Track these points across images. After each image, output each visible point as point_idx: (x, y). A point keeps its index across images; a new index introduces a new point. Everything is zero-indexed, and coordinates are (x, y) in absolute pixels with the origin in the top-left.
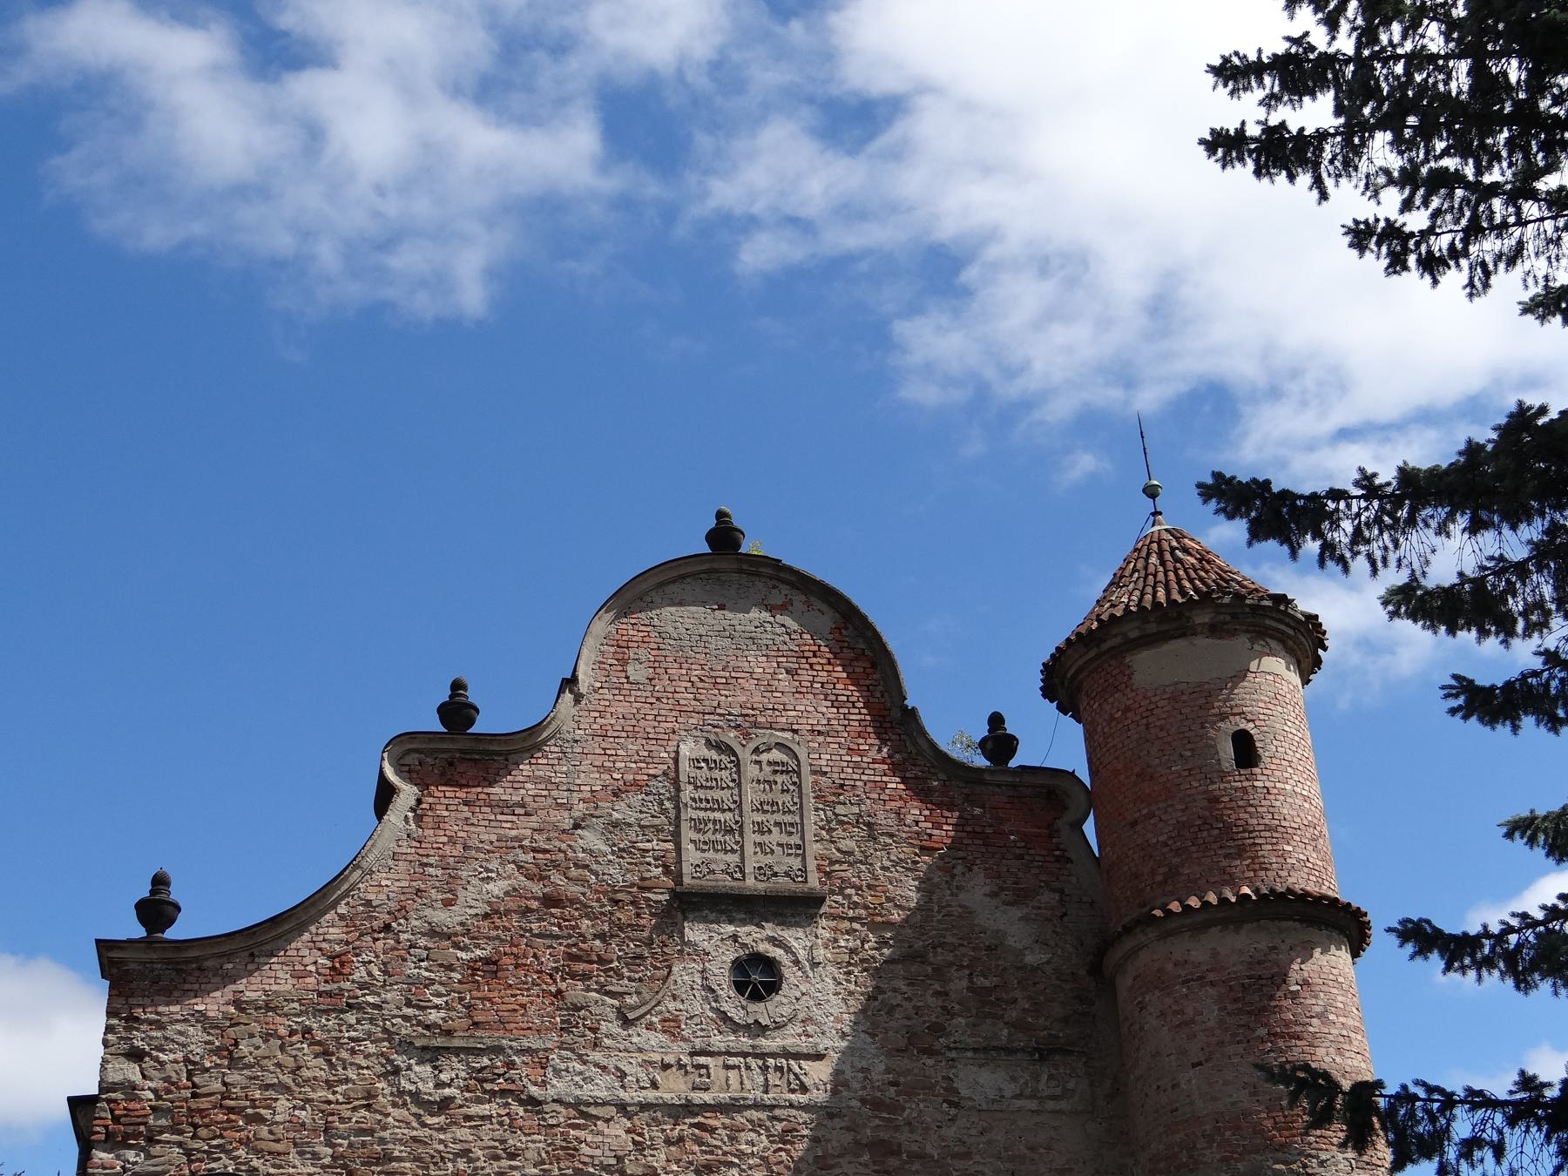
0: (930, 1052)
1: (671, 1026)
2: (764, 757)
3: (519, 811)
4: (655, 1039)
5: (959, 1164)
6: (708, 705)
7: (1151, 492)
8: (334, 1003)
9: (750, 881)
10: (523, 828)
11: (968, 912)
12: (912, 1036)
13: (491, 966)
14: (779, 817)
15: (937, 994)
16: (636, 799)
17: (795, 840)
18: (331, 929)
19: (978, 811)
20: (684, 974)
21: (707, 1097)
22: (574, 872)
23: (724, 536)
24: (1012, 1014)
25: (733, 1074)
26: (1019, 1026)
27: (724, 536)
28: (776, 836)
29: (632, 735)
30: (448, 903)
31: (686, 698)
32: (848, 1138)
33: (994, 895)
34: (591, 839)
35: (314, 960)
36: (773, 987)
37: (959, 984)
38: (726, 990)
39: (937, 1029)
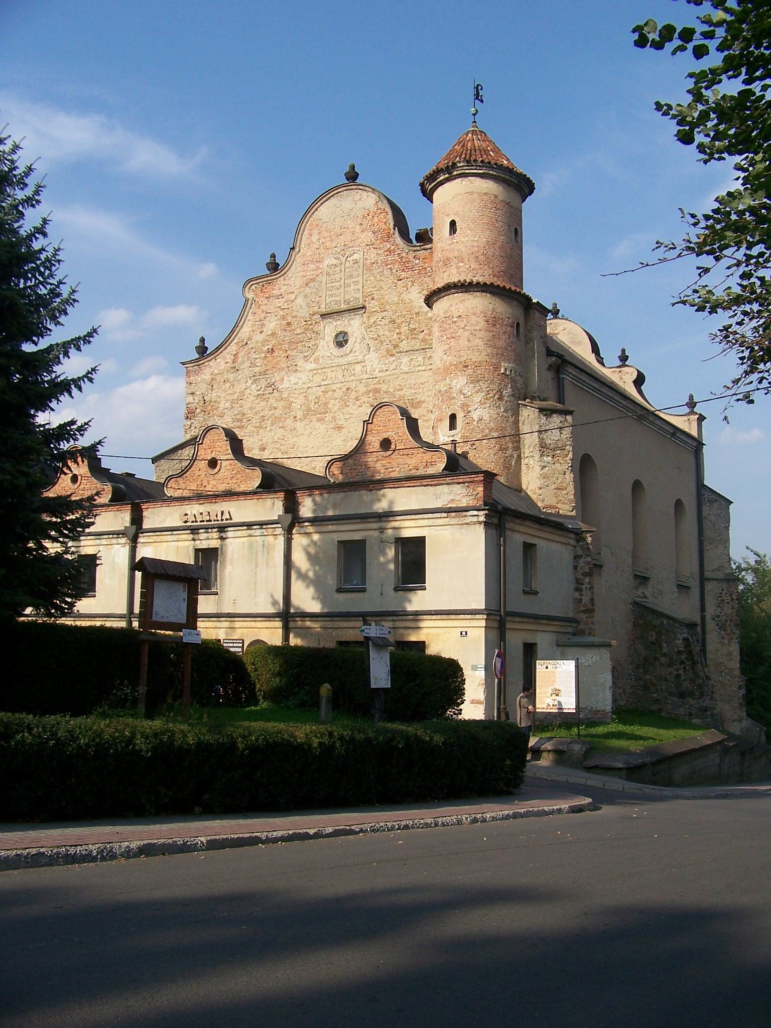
0: (392, 355)
1: (316, 361)
5: (398, 393)
6: (335, 244)
8: (235, 369)
10: (279, 303)
11: (411, 301)
12: (388, 351)
14: (355, 280)
16: (312, 284)
18: (233, 348)
19: (417, 261)
20: (322, 343)
22: (295, 313)
25: (334, 374)
26: (424, 340)
28: (353, 287)
29: (312, 262)
31: (328, 244)
32: (365, 389)
33: (420, 293)
34: (300, 301)
35: (230, 358)
36: (346, 341)
37: (404, 329)
38: (332, 345)
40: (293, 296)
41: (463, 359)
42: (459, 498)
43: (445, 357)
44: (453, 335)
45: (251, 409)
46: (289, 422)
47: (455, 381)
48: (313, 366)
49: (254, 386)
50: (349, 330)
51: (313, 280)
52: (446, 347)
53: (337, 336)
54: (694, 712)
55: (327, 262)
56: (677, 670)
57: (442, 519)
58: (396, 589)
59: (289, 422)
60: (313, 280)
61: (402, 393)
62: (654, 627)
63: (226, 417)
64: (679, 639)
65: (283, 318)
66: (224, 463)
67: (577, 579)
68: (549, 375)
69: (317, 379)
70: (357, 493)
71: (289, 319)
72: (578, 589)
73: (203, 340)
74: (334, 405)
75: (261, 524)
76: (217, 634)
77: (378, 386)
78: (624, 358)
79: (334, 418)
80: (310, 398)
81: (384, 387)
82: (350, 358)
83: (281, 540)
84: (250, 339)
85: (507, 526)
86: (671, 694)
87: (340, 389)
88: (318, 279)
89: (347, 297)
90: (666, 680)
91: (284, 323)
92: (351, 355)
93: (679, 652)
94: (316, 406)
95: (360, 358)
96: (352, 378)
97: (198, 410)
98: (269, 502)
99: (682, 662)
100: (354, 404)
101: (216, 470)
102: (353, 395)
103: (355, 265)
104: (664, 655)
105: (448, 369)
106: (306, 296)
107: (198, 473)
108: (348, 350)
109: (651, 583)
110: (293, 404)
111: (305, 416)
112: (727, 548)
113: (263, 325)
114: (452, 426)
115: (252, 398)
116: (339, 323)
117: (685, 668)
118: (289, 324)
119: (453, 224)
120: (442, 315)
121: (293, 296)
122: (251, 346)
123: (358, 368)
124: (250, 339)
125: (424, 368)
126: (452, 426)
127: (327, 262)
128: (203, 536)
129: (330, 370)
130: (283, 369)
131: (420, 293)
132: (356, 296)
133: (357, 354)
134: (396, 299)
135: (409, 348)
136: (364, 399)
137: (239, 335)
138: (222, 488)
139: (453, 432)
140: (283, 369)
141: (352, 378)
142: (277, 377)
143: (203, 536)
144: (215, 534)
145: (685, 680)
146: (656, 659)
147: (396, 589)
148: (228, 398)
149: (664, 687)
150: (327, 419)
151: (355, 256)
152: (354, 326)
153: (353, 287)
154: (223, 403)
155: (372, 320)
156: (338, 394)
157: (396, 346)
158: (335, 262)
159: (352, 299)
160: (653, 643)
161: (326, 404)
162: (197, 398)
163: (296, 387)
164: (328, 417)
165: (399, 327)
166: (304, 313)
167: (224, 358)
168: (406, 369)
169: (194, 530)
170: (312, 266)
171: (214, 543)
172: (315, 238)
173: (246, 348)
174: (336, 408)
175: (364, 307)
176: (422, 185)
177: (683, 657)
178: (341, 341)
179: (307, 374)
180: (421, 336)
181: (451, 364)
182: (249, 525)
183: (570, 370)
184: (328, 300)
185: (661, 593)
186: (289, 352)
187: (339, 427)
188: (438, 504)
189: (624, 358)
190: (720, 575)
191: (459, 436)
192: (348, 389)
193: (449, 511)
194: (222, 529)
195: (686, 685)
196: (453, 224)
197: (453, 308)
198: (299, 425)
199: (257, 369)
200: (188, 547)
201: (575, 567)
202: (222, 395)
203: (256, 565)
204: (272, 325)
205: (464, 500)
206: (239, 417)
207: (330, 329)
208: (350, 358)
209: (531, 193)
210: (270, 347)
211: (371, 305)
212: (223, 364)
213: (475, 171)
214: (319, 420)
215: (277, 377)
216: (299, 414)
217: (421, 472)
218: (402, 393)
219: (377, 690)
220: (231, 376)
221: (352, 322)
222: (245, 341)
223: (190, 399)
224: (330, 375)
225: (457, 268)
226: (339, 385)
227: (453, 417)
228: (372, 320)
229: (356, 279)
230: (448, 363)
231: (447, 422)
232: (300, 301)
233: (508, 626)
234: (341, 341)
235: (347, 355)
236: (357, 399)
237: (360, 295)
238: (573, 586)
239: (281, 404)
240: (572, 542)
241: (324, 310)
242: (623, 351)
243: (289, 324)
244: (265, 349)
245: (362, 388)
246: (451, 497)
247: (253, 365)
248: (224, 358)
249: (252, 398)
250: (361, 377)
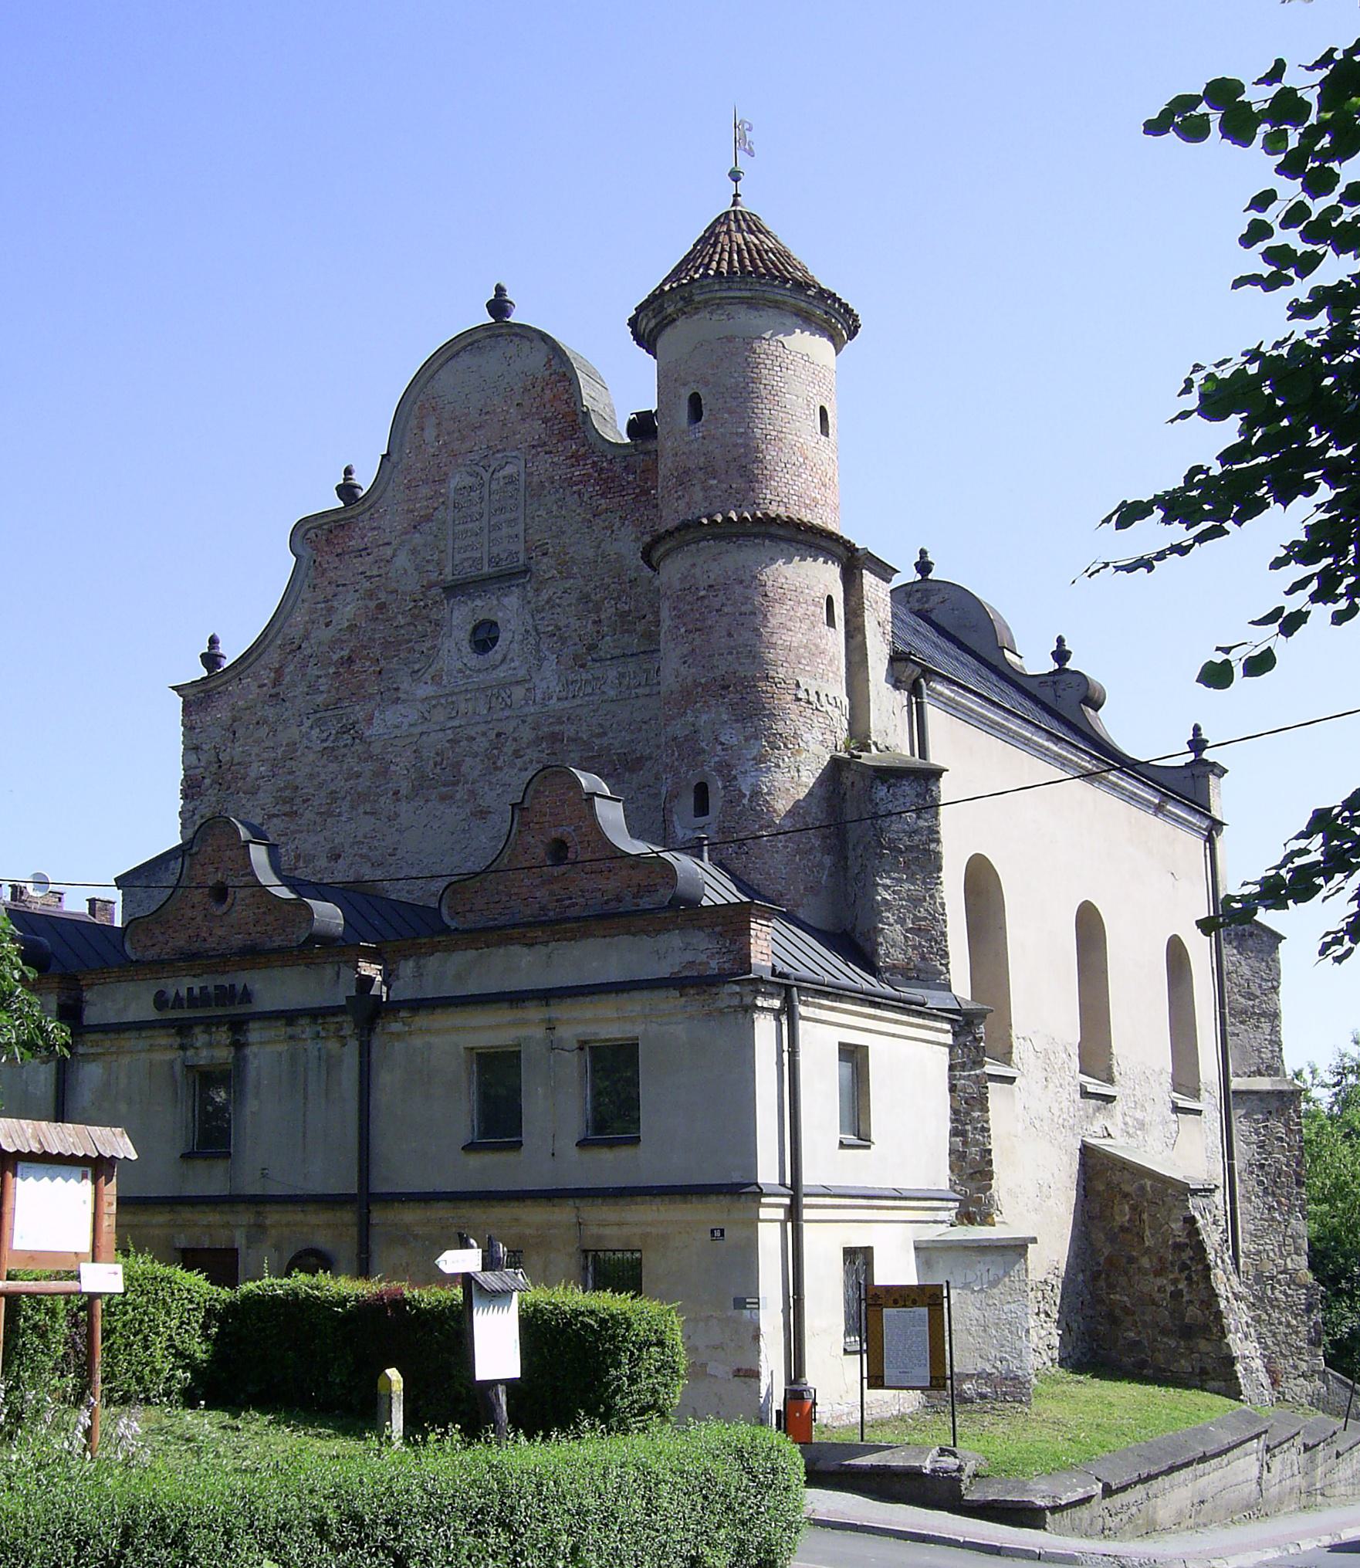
1: (436, 679)
2: (502, 473)
3: (364, 553)
4: (429, 690)
5: (597, 741)
6: (467, 445)
7: (735, 176)
9: (486, 569)
12: (576, 657)
13: (350, 660)
15: (595, 622)
16: (425, 527)
17: (512, 532)
18: (273, 657)
19: (631, 478)
20: (448, 644)
21: (456, 723)
22: (394, 585)
23: (499, 306)
24: (640, 627)
27: (499, 306)
30: (327, 625)
31: (456, 445)
32: (532, 736)
34: (403, 560)
35: (267, 677)
36: (496, 639)
37: (608, 611)
39: (592, 648)
40: (389, 551)
41: (718, 673)
42: (703, 957)
43: (683, 669)
44: (699, 625)
45: (311, 776)
46: (385, 802)
47: (705, 717)
48: (429, 690)
49: (315, 732)
50: (499, 616)
51: (428, 518)
52: (685, 649)
53: (476, 629)
54: (1209, 1368)
55: (454, 482)
56: (1175, 1282)
57: (669, 1001)
58: (582, 1144)
59: (385, 802)
60: (428, 518)
61: (605, 741)
62: (1126, 1195)
63: (261, 794)
64: (1177, 1220)
65: (371, 595)
66: (241, 894)
67: (955, 1111)
68: (902, 697)
69: (439, 715)
70: (502, 951)
71: (383, 597)
72: (954, 1133)
73: (213, 641)
74: (471, 768)
75: (316, 1014)
76: (232, 1239)
77: (557, 728)
78: (1061, 655)
79: (472, 793)
80: (425, 754)
81: (569, 730)
82: (501, 673)
83: (353, 1047)
84: (306, 637)
85: (802, 1010)
86: (1164, 1332)
87: (484, 734)
88: (438, 515)
89: (495, 550)
90: (1154, 1303)
91: (372, 604)
92: (504, 667)
93: (1178, 1247)
94: (438, 770)
95: (522, 673)
96: (507, 713)
97: (207, 781)
98: (329, 971)
99: (1184, 1267)
100: (512, 765)
101: (225, 908)
102: (509, 748)
103: (510, 488)
104: (1148, 1251)
105: (689, 693)
106: (414, 552)
107: (189, 913)
108: (499, 657)
109: (1118, 1107)
110: (393, 768)
111: (416, 790)
112: (1275, 1031)
113: (331, 610)
114: (702, 807)
115: (311, 757)
116: (478, 602)
117: (1189, 1278)
118: (381, 607)
119: (695, 401)
120: (677, 585)
121: (389, 551)
122: (309, 651)
123: (519, 692)
124: (306, 637)
125: (647, 690)
126: (702, 807)
127: (454, 482)
128: (200, 1038)
129: (462, 697)
130: (371, 696)
131: (637, 539)
132: (514, 548)
133: (517, 664)
134: (590, 553)
135: (618, 652)
136: (531, 754)
137: (286, 630)
138: (237, 940)
139: (702, 820)
140: (371, 696)
141: (507, 713)
142: (359, 712)
143: (200, 1038)
144: (223, 1035)
145: (1191, 1302)
146: (1131, 1260)
147: (582, 1144)
148: (265, 755)
149: (1147, 1318)
150: (458, 796)
151: (509, 470)
152: (509, 610)
153: (505, 531)
154: (255, 765)
155: (545, 596)
156: (482, 744)
157: (592, 648)
158: (469, 481)
159: (504, 556)
160: (1123, 1229)
161: (458, 765)
162: (204, 758)
163: (397, 732)
164: (461, 793)
165: (598, 609)
166: (411, 584)
167: (256, 676)
168: (612, 693)
169: (183, 1028)
170: (425, 491)
171: (223, 1054)
172: (430, 433)
173: (299, 656)
174: (477, 773)
175: (527, 571)
176: (633, 323)
177: (1184, 1256)
178: (484, 637)
179: (419, 706)
180: (640, 627)
181: (696, 684)
182: (289, 1017)
183: (939, 688)
184: (458, 557)
185: (1142, 1125)
186: (383, 663)
187: (481, 812)
188: (664, 970)
189: (1061, 655)
190: (1264, 1084)
191: (714, 827)
192: (498, 735)
193: (677, 983)
194: (238, 1026)
195: (1193, 1312)
196: (695, 401)
197: (697, 571)
198: (404, 806)
199: (320, 699)
200: (172, 1063)
201: (953, 1089)
202: (255, 750)
203: (306, 1098)
204: (348, 609)
205: (713, 964)
206: (287, 793)
207: (462, 616)
208: (501, 673)
209: (852, 334)
210: (345, 653)
211: (545, 566)
212: (254, 688)
213: (738, 294)
214: (443, 798)
215: (359, 712)
216: (405, 788)
217: (628, 905)
218: (605, 741)
219: (493, 1384)
220: (270, 713)
221: (506, 601)
222: (297, 642)
223: (193, 759)
224: (462, 707)
225: (705, 489)
226: (482, 728)
227: (702, 792)
228: (545, 596)
229: (513, 515)
230: (689, 680)
231: (689, 801)
232: (403, 560)
233: (807, 1214)
234: (484, 637)
235: (495, 667)
236: (517, 754)
237: (521, 547)
238: (948, 1126)
239: (369, 767)
240: (948, 1039)
241: (450, 578)
242: (1060, 641)
243: (381, 607)
244: (335, 657)
245: (526, 734)
246: (689, 956)
247: (313, 689)
248: (256, 676)
249: (311, 757)
250: (526, 710)
